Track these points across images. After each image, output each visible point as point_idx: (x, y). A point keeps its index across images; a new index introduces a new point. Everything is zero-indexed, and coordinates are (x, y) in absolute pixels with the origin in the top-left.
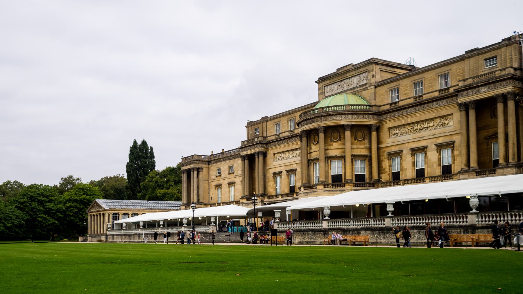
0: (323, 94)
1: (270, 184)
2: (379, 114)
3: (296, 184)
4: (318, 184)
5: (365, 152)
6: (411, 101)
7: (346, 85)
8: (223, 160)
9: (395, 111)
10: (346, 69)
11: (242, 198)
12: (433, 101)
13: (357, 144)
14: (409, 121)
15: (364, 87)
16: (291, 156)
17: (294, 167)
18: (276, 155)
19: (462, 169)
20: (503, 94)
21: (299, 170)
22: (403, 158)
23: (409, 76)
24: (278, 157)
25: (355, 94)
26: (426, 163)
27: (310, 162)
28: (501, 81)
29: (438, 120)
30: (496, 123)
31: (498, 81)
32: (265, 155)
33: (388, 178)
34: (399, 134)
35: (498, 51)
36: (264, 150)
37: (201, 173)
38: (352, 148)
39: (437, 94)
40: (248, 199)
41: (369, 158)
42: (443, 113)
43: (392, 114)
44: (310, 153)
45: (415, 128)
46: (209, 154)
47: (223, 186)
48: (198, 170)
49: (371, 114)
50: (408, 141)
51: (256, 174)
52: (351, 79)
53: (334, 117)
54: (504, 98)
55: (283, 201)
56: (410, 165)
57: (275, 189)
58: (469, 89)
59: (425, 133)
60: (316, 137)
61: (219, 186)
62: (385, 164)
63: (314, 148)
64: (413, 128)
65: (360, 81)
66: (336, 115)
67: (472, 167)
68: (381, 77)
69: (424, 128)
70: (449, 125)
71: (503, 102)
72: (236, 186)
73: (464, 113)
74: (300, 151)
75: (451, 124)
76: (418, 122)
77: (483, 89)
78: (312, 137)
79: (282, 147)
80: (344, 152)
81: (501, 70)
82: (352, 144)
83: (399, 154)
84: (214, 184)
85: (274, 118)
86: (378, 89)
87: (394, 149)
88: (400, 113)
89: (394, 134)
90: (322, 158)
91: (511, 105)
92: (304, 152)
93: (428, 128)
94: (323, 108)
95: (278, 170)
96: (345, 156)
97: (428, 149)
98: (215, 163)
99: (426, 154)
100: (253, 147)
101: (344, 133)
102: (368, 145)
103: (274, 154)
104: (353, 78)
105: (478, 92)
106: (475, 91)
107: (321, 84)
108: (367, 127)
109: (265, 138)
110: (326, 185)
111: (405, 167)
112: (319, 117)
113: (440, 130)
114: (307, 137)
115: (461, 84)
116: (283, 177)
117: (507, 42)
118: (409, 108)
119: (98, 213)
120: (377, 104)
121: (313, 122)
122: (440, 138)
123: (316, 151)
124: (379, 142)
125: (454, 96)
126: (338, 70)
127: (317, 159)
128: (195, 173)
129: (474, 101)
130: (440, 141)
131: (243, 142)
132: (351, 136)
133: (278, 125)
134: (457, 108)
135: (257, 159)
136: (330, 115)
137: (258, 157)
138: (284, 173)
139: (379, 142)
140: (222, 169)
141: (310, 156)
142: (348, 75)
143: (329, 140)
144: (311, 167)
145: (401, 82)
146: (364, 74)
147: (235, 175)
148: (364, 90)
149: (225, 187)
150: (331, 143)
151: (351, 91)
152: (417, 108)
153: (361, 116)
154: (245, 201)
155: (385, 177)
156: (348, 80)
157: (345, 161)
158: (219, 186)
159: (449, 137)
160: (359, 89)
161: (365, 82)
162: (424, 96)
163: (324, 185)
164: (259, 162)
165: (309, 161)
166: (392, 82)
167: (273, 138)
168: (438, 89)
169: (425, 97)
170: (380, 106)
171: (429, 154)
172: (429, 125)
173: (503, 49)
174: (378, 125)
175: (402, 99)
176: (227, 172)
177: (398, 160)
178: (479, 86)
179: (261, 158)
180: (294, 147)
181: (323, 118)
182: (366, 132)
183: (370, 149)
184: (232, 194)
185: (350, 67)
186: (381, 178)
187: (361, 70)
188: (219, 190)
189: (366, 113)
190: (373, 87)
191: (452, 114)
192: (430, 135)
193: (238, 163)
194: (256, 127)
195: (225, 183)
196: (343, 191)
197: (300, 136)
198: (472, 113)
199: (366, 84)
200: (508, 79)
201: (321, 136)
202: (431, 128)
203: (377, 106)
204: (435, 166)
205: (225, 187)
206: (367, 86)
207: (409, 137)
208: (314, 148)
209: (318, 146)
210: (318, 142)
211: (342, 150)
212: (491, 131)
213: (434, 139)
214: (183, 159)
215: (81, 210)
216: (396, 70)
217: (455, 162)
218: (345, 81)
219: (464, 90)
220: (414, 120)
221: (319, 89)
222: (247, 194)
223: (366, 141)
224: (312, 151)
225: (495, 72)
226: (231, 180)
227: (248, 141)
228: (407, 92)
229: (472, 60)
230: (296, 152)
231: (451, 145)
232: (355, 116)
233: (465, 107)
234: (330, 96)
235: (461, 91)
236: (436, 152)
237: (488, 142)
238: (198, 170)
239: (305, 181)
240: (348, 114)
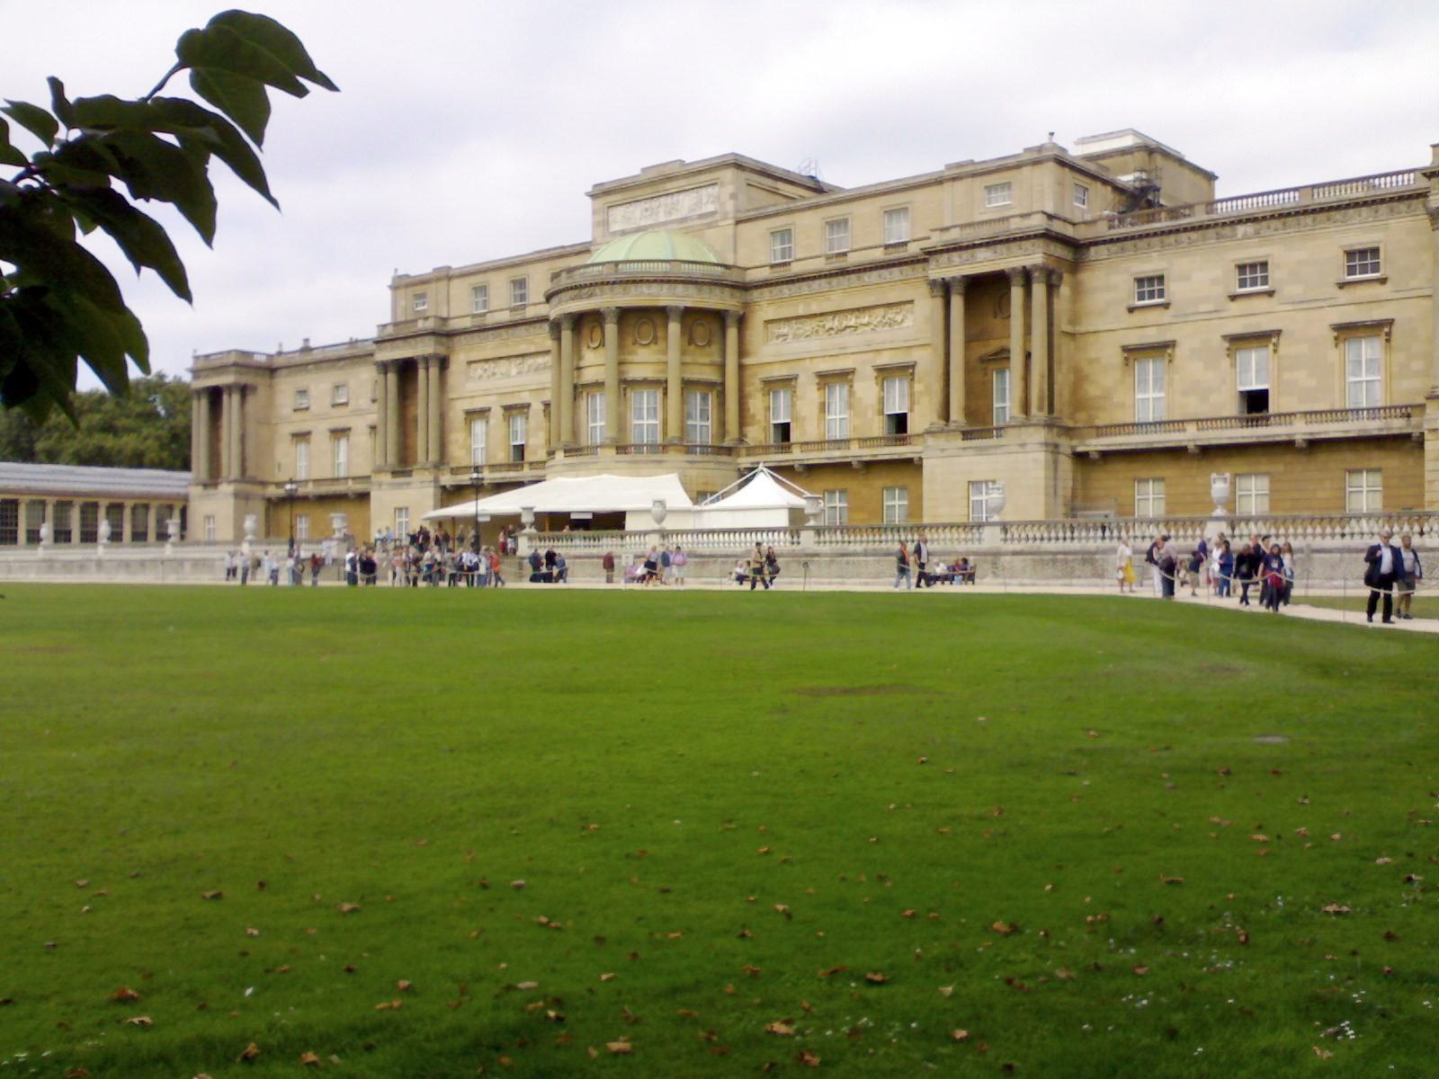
0: (603, 224)
1: (457, 437)
2: (745, 287)
3: (527, 441)
4: (602, 446)
5: (710, 375)
6: (819, 265)
7: (663, 209)
9: (782, 283)
10: (667, 171)
11: (378, 471)
12: (871, 269)
14: (815, 309)
15: (709, 220)
16: (514, 371)
17: (524, 398)
18: (473, 366)
19: (932, 424)
20: (1024, 267)
21: (537, 407)
22: (799, 391)
23: (818, 206)
24: (480, 372)
25: (688, 231)
26: (850, 406)
27: (578, 390)
28: (1021, 239)
29: (880, 312)
30: (1007, 327)
31: (1015, 240)
32: (444, 363)
33: (762, 437)
34: (790, 337)
35: (1015, 172)
36: (442, 351)
37: (251, 400)
38: (683, 364)
39: (878, 255)
40: (395, 474)
41: (719, 388)
42: (893, 297)
43: (776, 290)
44: (579, 368)
45: (827, 327)
46: (273, 351)
47: (313, 438)
48: (244, 391)
49: (727, 286)
50: (810, 355)
51: (420, 411)
52: (676, 197)
53: (644, 288)
54: (1027, 276)
56: (815, 410)
57: (469, 450)
58: (955, 249)
59: (851, 340)
60: (597, 334)
61: (301, 436)
62: (756, 404)
63: (589, 357)
64: (824, 326)
65: (699, 203)
66: (648, 281)
67: (954, 422)
69: (847, 327)
70: (904, 325)
71: (1023, 286)
72: (352, 438)
73: (939, 302)
74: (547, 359)
75: (908, 323)
76: (835, 313)
77: (982, 254)
78: (586, 332)
79: (490, 346)
80: (665, 371)
81: (1023, 216)
82: (683, 353)
83: (788, 382)
84: (286, 430)
85: (465, 274)
86: (741, 226)
87: (778, 372)
88: (795, 287)
89: (778, 337)
90: (611, 383)
91: (1039, 290)
92: (566, 365)
93: (856, 327)
94: (617, 263)
95: (479, 404)
96: (666, 381)
97: (856, 377)
99: (851, 386)
101: (666, 327)
102: (717, 359)
103: (470, 363)
104: (681, 196)
105: (973, 261)
106: (965, 254)
107: (602, 201)
108: (715, 317)
109: (445, 320)
110: (622, 449)
111: (803, 414)
112: (608, 283)
113: (885, 336)
114: (573, 330)
115: (937, 240)
116: (492, 421)
117: (1035, 155)
118: (814, 278)
120: (740, 264)
121: (591, 295)
122: (885, 353)
123: (596, 362)
124: (742, 352)
125: (918, 261)
126: (644, 170)
127: (599, 385)
128: (236, 398)
129: (964, 276)
130: (885, 359)
131: (384, 326)
132: (683, 333)
133: (481, 290)
134: (925, 289)
135: (421, 373)
136: (634, 282)
137: (427, 369)
138: (497, 414)
139: (742, 352)
140: (313, 391)
141: (579, 377)
143: (629, 341)
144: (583, 403)
145: (796, 218)
146: (710, 190)
147: (350, 407)
148: (709, 226)
149: (321, 439)
151: (675, 226)
152: (835, 281)
153: (706, 288)
154: (387, 478)
155: (755, 434)
156: (669, 199)
157: (665, 393)
158: (301, 436)
161: (711, 208)
162: (850, 255)
164: (426, 379)
165: (575, 387)
166: (777, 214)
167: (467, 323)
168: (882, 243)
169: (854, 259)
170: (746, 269)
171: (857, 386)
172: (859, 321)
173: (1026, 170)
174: (741, 313)
175: (799, 256)
176: (328, 401)
177: (783, 397)
178: (974, 246)
179: (434, 371)
181: (618, 288)
182: (715, 327)
183: (722, 367)
184: (342, 458)
185: (676, 169)
186: (745, 436)
187: (703, 178)
188: (302, 447)
189: (717, 283)
190: (731, 221)
191: (911, 302)
192: (862, 344)
193: (364, 383)
194: (419, 289)
195: (320, 430)
196: (660, 462)
197: (556, 327)
198: (957, 303)
199: (713, 213)
200: (1036, 236)
201: (611, 329)
203: (739, 268)
204: (870, 414)
205: (321, 439)
206: (717, 217)
207: (813, 345)
208: (589, 357)
209: (601, 350)
210: (602, 344)
211: (661, 367)
212: (994, 346)
213: (870, 356)
214: (197, 358)
216: (780, 185)
217: (916, 407)
218: (662, 200)
219: (941, 251)
221: (594, 212)
222: (392, 459)
223: (715, 348)
224: (582, 364)
225: (1007, 219)
226: (340, 423)
227: (396, 324)
228: (811, 242)
229: (959, 185)
230: (530, 361)
231: (906, 370)
232: (691, 289)
233: (945, 288)
234: (624, 233)
235: (936, 252)
236: (874, 381)
237: (986, 369)
238: (244, 391)
239: (566, 437)
240: (676, 282)
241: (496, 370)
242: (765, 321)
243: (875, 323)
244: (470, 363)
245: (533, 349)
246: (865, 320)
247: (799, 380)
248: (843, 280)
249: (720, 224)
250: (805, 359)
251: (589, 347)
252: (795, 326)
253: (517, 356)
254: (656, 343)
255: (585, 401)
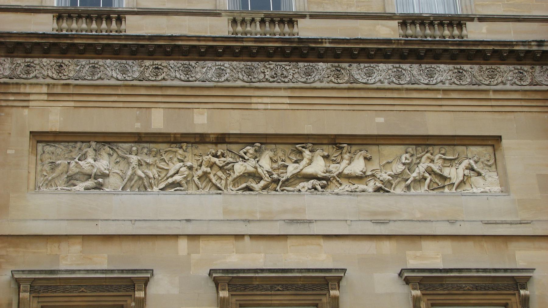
14: (201, 120)
34: (114, 181)
45: (240, 168)
76: (261, 141)
93: (326, 181)
159: (487, 245)
168: (400, 11)
202: (346, 186)
213: (387, 246)
220: (234, 122)
242: (31, 132)
243: (385, 176)
246: (358, 166)
247: (153, 289)
248: (294, 71)
250: (177, 236)
252: (134, 159)
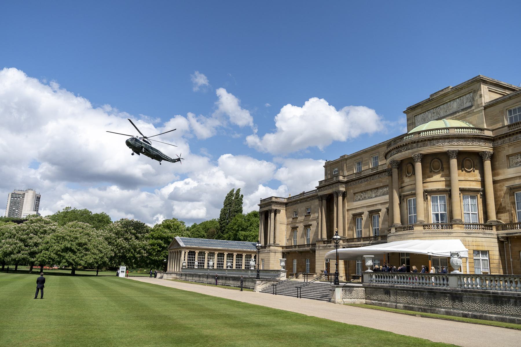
0: (411, 124)
8: (300, 202)
13: (465, 175)
16: (374, 195)
24: (359, 197)
43: (512, 138)
44: (402, 188)
55: (365, 245)
68: (490, 97)
86: (487, 110)
98: (292, 205)
100: (331, 186)
103: (355, 194)
104: (452, 102)
114: (398, 169)
119: (176, 250)
126: (431, 96)
128: (273, 214)
135: (335, 198)
137: (337, 198)
142: (445, 99)
143: (428, 171)
150: (430, 174)
156: (446, 105)
160: (460, 113)
163: (424, 226)
180: (377, 185)
182: (477, 161)
183: (483, 182)
206: (473, 108)
215: (164, 248)
218: (441, 107)
224: (404, 185)
241: (366, 196)
244: (355, 194)
245: (381, 185)
249: (475, 111)
251: (406, 176)
253: (375, 189)
254: (443, 171)
255: (405, 203)
